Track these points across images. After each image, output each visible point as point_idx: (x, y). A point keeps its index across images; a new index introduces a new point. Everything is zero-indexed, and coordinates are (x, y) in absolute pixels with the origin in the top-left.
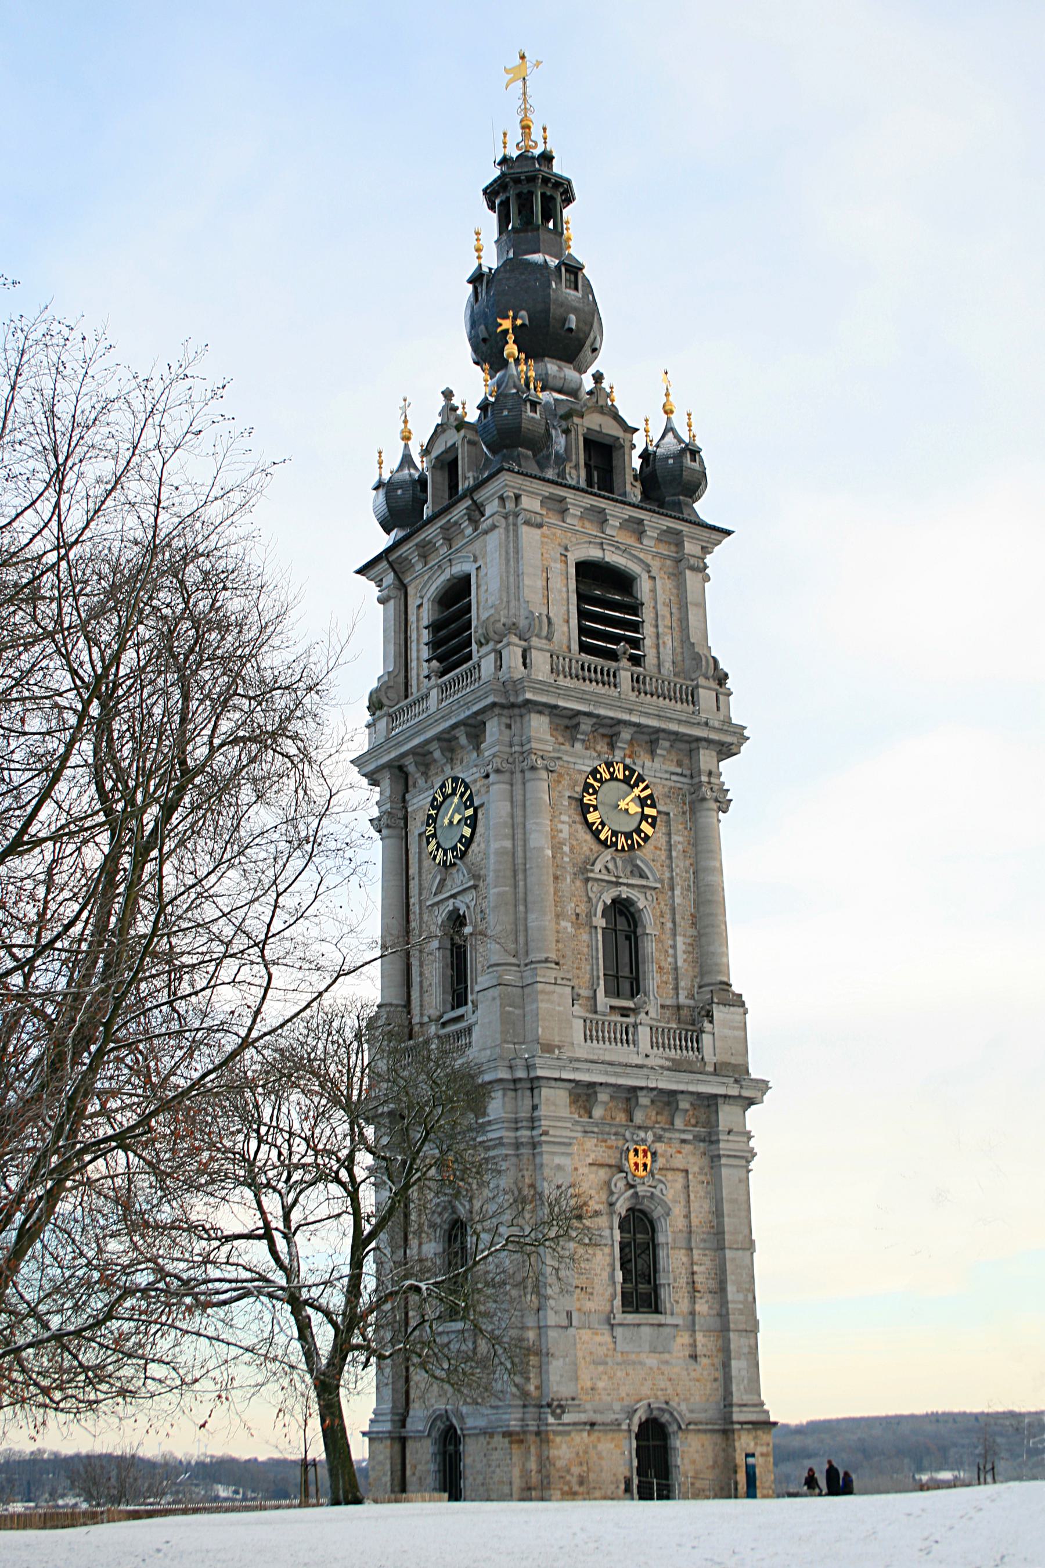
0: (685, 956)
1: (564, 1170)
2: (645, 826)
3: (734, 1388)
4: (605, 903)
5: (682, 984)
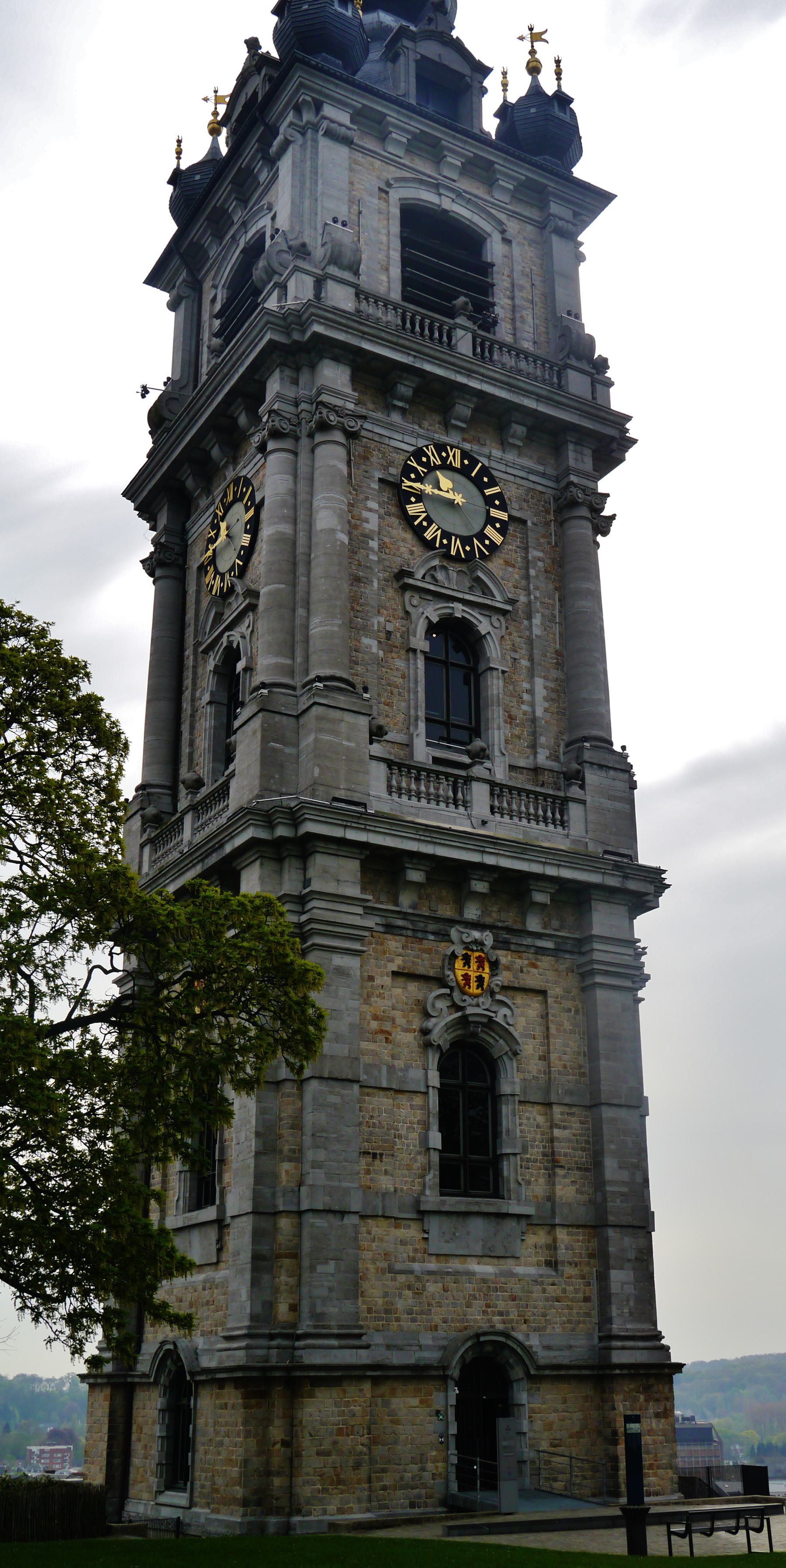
0: (546, 705)
1: (348, 975)
2: (489, 531)
3: (614, 1312)
4: (430, 622)
5: (543, 740)
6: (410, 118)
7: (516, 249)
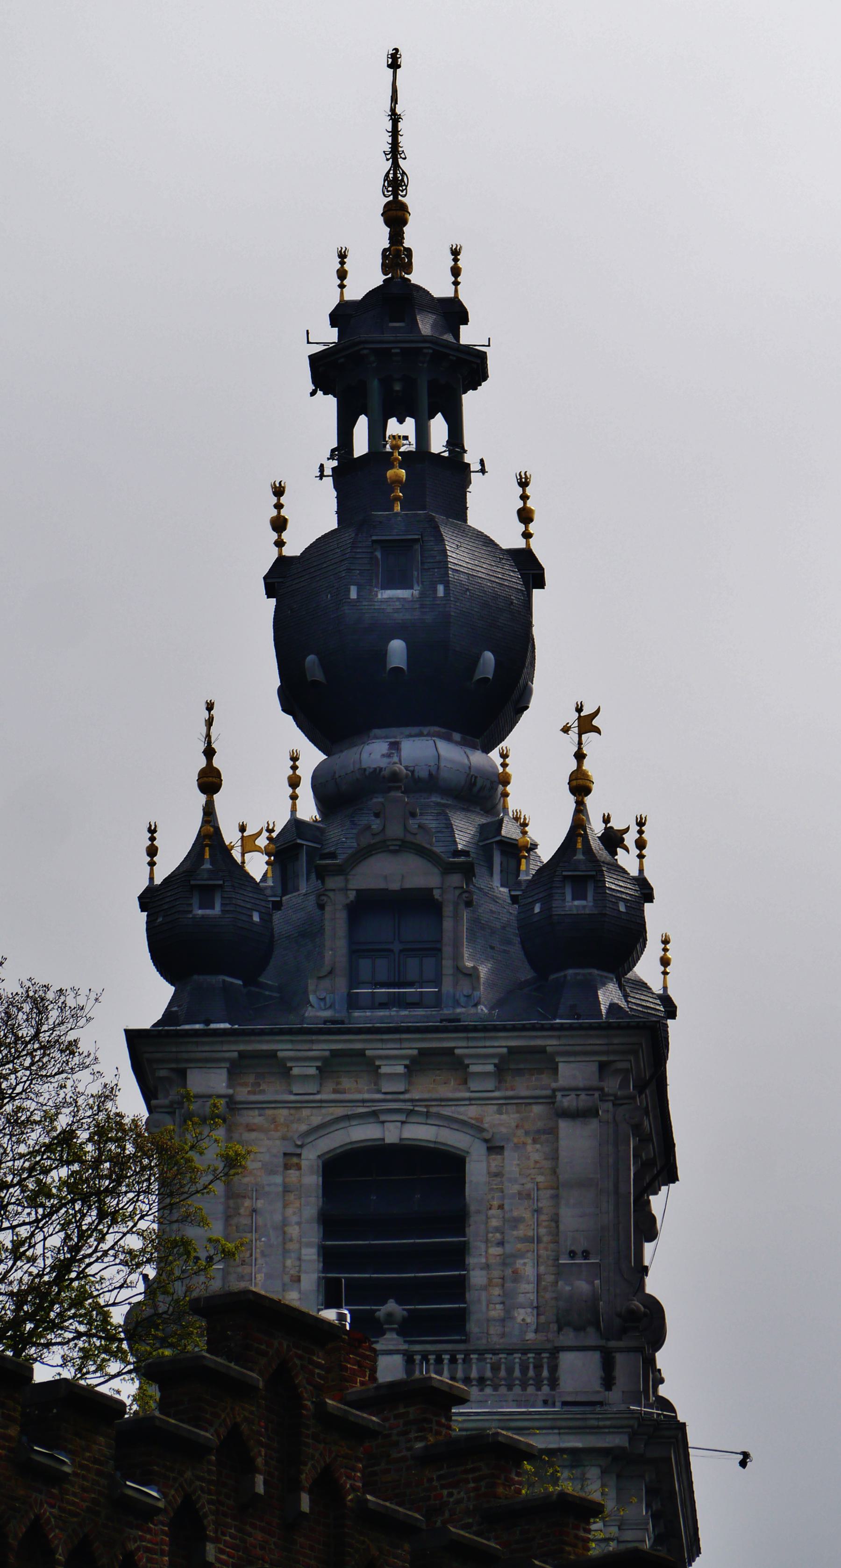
6: (312, 1042)
7: (511, 1162)
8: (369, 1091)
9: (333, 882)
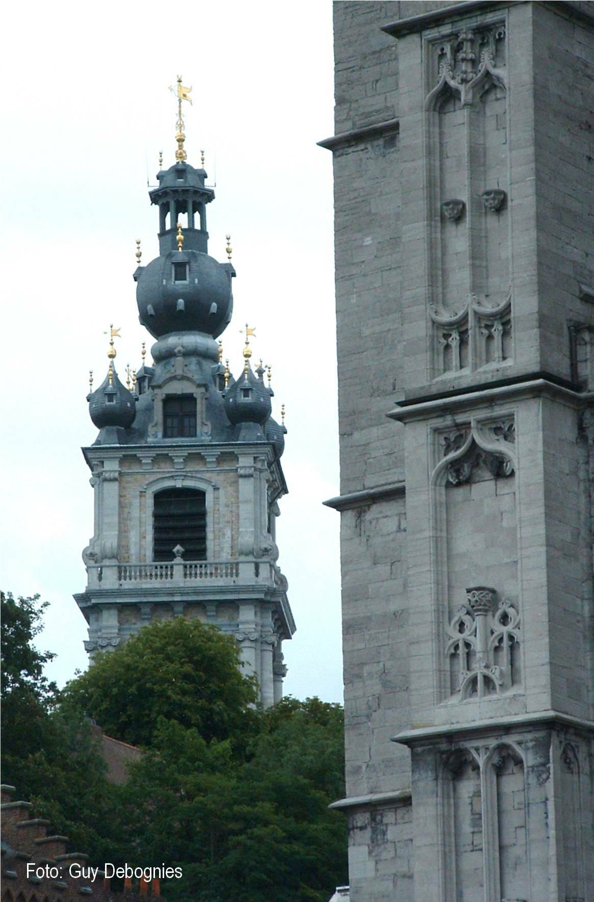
8: (171, 468)
9: (156, 391)
